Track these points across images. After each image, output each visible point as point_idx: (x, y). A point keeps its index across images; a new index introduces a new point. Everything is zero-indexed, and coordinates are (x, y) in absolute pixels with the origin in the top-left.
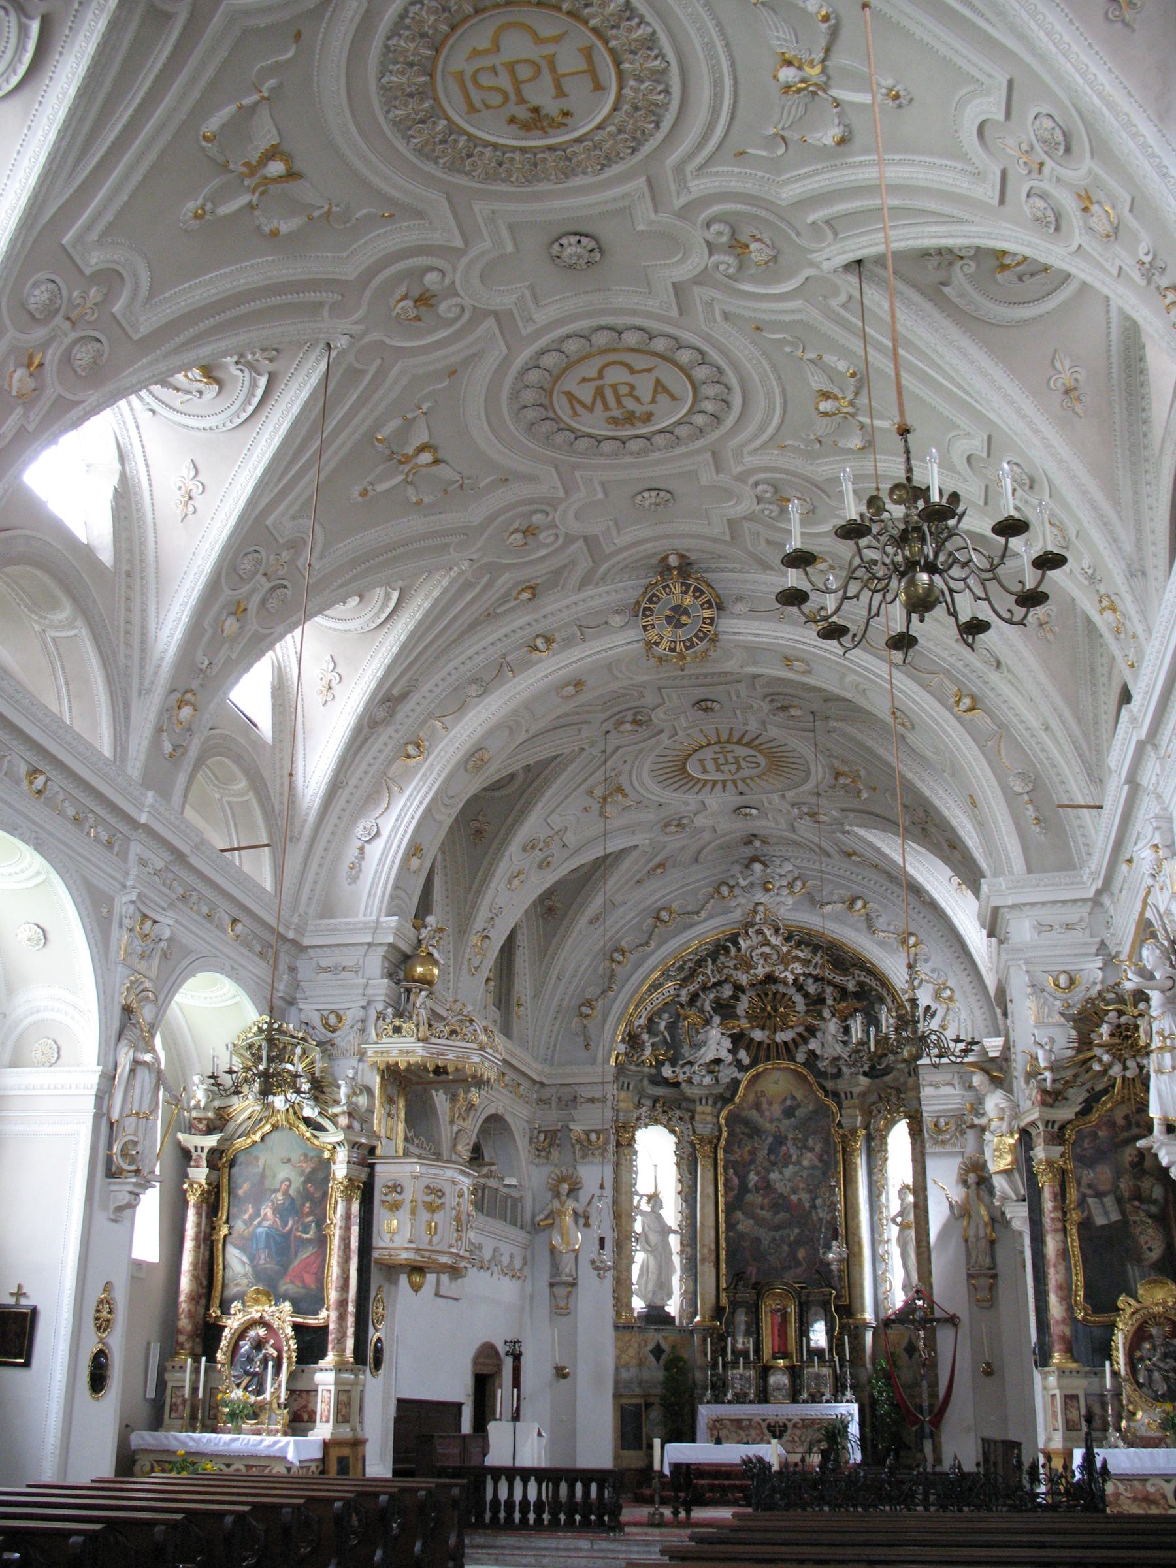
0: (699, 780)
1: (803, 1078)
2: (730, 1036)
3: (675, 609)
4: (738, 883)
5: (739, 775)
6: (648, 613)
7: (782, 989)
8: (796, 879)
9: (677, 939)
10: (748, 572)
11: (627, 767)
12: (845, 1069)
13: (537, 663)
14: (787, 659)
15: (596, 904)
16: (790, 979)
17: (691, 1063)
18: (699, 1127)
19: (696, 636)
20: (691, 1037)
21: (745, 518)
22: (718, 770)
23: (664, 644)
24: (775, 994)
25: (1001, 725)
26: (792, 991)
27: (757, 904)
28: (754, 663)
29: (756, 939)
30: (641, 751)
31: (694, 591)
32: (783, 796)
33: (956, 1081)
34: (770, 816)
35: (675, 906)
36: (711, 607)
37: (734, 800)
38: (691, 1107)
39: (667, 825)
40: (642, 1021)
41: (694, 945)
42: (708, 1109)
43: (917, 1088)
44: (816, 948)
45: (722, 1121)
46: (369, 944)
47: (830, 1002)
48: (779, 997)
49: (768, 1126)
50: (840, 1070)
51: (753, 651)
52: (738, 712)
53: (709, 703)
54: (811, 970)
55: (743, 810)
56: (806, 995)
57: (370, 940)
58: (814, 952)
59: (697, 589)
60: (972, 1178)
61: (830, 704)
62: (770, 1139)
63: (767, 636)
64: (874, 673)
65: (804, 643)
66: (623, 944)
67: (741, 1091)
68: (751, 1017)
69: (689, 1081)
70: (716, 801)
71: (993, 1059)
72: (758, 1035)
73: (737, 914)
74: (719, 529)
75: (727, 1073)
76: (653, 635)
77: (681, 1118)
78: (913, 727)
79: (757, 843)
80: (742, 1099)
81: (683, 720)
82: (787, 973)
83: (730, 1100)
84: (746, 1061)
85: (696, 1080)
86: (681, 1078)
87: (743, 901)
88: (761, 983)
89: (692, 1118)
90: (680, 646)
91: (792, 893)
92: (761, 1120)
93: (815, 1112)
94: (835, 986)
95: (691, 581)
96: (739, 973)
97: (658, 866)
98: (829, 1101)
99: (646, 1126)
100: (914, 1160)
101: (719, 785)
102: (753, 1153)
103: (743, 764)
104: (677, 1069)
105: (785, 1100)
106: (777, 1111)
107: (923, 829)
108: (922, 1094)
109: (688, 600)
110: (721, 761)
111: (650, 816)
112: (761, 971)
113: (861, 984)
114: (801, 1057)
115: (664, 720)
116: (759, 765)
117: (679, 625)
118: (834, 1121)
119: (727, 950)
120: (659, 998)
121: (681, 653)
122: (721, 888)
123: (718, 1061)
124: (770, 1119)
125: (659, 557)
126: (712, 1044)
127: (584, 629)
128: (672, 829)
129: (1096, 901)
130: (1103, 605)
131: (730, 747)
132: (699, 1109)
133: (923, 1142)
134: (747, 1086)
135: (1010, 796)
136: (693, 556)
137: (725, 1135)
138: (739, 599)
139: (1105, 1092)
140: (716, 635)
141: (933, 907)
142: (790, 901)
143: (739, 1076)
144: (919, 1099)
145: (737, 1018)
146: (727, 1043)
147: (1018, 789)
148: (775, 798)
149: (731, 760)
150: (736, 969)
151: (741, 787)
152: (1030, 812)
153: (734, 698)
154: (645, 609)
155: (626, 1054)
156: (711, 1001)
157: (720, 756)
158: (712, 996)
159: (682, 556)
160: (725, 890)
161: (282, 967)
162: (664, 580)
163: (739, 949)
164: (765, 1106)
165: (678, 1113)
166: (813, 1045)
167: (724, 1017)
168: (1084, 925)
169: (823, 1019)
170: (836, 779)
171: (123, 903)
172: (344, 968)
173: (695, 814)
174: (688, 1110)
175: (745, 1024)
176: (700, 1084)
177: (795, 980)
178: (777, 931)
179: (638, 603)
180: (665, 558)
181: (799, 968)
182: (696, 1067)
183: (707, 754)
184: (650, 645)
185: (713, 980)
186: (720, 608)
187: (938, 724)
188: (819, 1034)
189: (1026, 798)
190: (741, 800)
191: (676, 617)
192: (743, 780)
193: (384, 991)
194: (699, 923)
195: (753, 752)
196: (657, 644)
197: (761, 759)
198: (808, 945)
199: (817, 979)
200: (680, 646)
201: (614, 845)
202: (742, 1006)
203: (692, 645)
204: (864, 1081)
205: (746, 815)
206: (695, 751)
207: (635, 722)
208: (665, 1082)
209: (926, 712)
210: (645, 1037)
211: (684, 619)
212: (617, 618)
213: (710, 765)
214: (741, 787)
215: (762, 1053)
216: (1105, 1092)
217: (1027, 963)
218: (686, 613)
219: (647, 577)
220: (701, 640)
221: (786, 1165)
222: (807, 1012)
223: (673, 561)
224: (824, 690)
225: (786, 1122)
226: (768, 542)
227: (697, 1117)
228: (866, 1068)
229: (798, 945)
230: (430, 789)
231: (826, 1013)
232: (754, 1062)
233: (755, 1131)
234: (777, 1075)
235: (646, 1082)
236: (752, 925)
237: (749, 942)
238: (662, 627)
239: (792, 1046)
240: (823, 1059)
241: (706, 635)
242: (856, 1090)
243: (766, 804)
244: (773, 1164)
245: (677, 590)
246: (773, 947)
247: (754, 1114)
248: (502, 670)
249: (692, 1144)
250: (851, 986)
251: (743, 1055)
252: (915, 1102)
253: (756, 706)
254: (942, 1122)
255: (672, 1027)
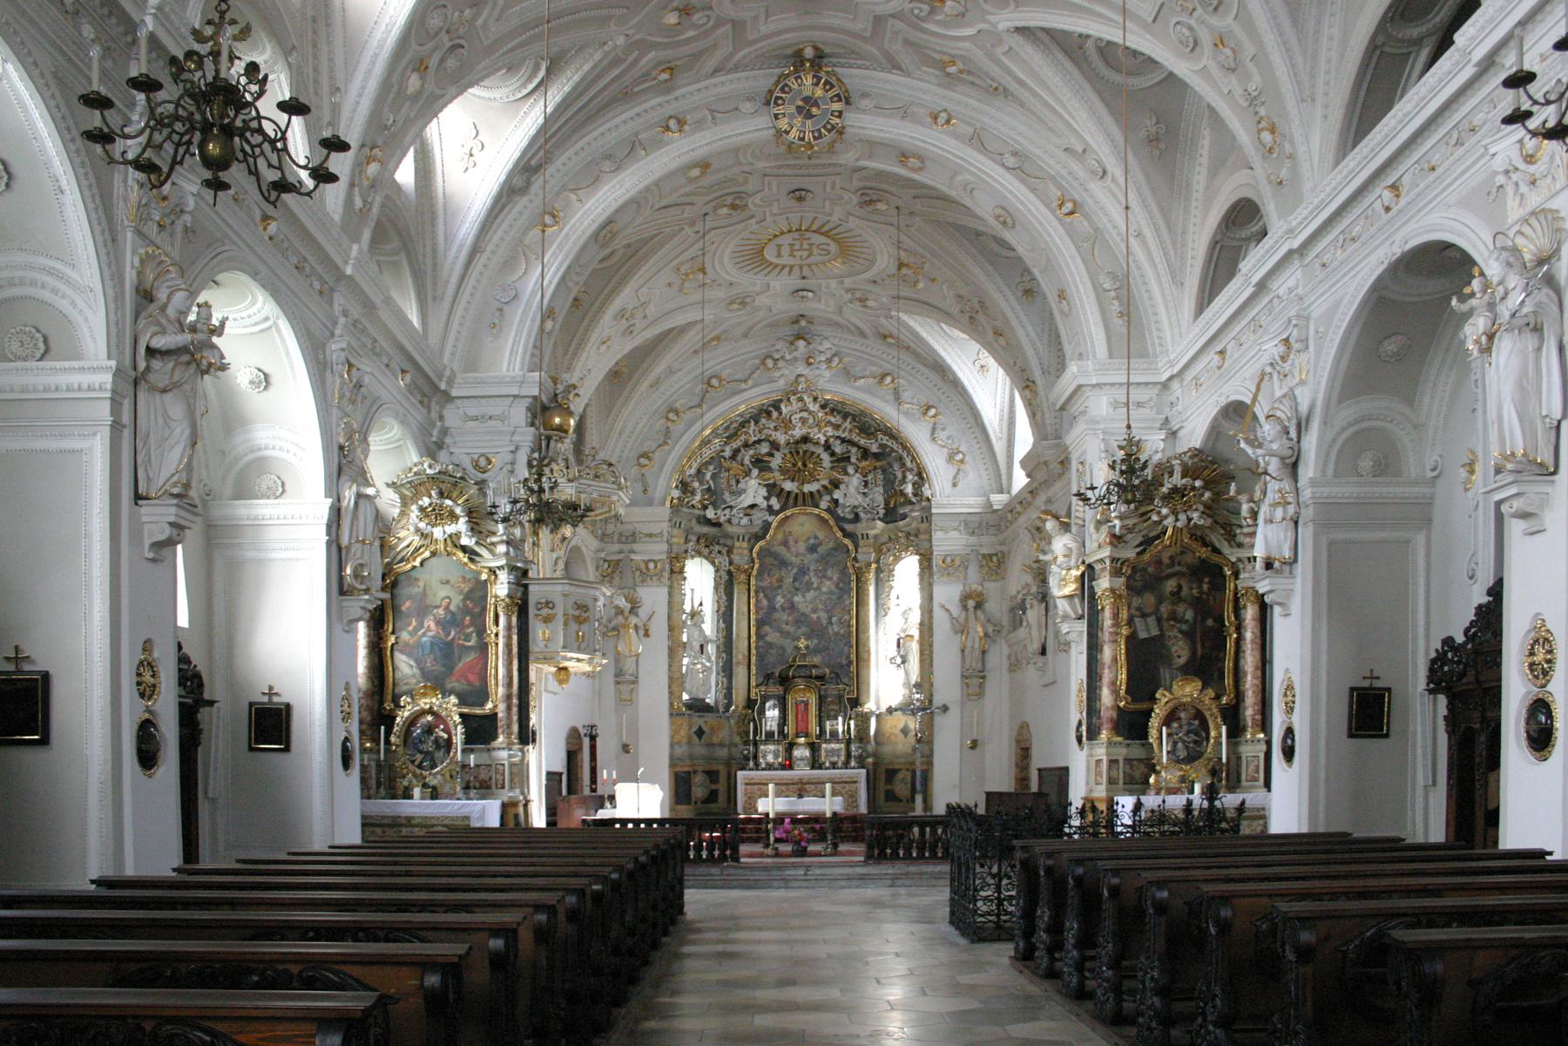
0: (771, 264)
1: (825, 521)
2: (766, 486)
3: (806, 100)
4: (783, 357)
5: (808, 261)
6: (780, 102)
7: (812, 448)
8: (834, 355)
9: (727, 402)
10: (875, 69)
11: (714, 246)
12: (862, 515)
13: (673, 142)
14: (903, 155)
15: (660, 368)
16: (823, 439)
17: (731, 507)
18: (736, 558)
19: (824, 127)
20: (730, 486)
21: (892, 16)
22: (792, 255)
23: (794, 134)
24: (805, 452)
25: (1097, 230)
26: (820, 450)
27: (799, 376)
28: (870, 157)
29: (796, 406)
30: (730, 233)
31: (825, 84)
32: (842, 282)
33: (962, 528)
34: (823, 298)
35: (724, 374)
36: (840, 100)
37: (794, 282)
38: (729, 542)
39: (731, 304)
40: (693, 471)
41: (742, 408)
42: (745, 545)
43: (929, 532)
44: (845, 417)
45: (754, 555)
46: (515, 396)
47: (853, 460)
48: (808, 454)
49: (794, 559)
50: (857, 515)
51: (873, 146)
52: (827, 203)
53: (803, 193)
54: (839, 433)
55: (801, 293)
56: (833, 454)
57: (516, 393)
58: (845, 417)
59: (826, 83)
60: (971, 603)
61: (918, 201)
62: (795, 570)
63: (890, 133)
64: (987, 175)
65: (924, 141)
66: (678, 405)
67: (771, 532)
68: (782, 470)
69: (729, 521)
70: (781, 283)
71: (996, 511)
72: (788, 486)
73: (781, 383)
74: (862, 25)
75: (759, 517)
76: (783, 124)
77: (719, 552)
78: (1014, 226)
79: (803, 323)
80: (772, 537)
81: (776, 204)
82: (820, 435)
83: (763, 537)
84: (777, 507)
85: (735, 521)
86: (722, 519)
87: (786, 372)
88: (797, 442)
89: (729, 552)
90: (809, 136)
91: (829, 368)
92: (788, 555)
93: (835, 549)
94: (859, 447)
95: (822, 74)
96: (778, 434)
97: (713, 339)
98: (846, 541)
99: (693, 557)
100: (922, 589)
101: (787, 269)
102: (780, 580)
103: (815, 251)
104: (719, 512)
105: (808, 539)
106: (802, 547)
107: (971, 317)
108: (934, 537)
109: (819, 92)
110: (796, 247)
111: (721, 294)
112: (798, 432)
113: (882, 446)
114: (824, 504)
115: (759, 206)
116: (829, 252)
117: (809, 116)
118: (849, 556)
119: (769, 414)
120: (707, 453)
121: (809, 142)
122: (767, 360)
123: (753, 506)
124: (796, 554)
125: (796, 48)
126: (751, 492)
127: (718, 112)
128: (735, 306)
129: (1165, 386)
130: (1261, 126)
131: (808, 235)
132: (737, 544)
133: (931, 575)
134: (777, 528)
135: (1099, 292)
136: (827, 50)
137: (757, 566)
138: (865, 95)
139: (1158, 537)
140: (843, 127)
141: (955, 384)
142: (827, 374)
143: (770, 519)
144: (930, 540)
145: (770, 469)
146: (764, 492)
147: (1107, 286)
148: (833, 283)
149: (805, 247)
150: (776, 429)
151: (806, 271)
152: (1116, 307)
153: (828, 189)
154: (777, 98)
155: (679, 498)
156: (752, 457)
157: (798, 242)
158: (751, 452)
159: (816, 48)
160: (770, 363)
161: (434, 415)
162: (796, 71)
163: (781, 413)
164: (791, 543)
165: (717, 548)
166: (837, 495)
167: (761, 470)
168: (1152, 404)
169: (846, 474)
170: (899, 269)
171: (336, 349)
172: (490, 418)
173: (758, 294)
174: (725, 545)
175: (777, 474)
176: (739, 524)
177: (826, 441)
178: (815, 399)
179: (771, 92)
180: (801, 50)
181: (830, 431)
182: (735, 511)
183: (786, 240)
184: (780, 133)
185: (754, 439)
186: (848, 102)
187: (1041, 223)
188: (842, 487)
189: (1113, 294)
190: (800, 283)
191: (806, 108)
192: (809, 266)
193: (531, 438)
194: (746, 390)
195: (828, 241)
196: (787, 132)
197: (833, 247)
198: (839, 412)
199: (843, 441)
200: (809, 136)
201: (680, 320)
202: (776, 462)
203: (820, 137)
204: (880, 524)
205: (803, 297)
206: (776, 236)
207: (733, 207)
208: (709, 522)
209: (1032, 214)
210: (696, 484)
211: (814, 110)
212: (748, 104)
213: (785, 250)
214: (805, 269)
215: (791, 501)
216: (1158, 537)
217: (1104, 432)
218: (816, 104)
219: (777, 67)
220: (829, 131)
221: (809, 591)
222: (832, 468)
223: (809, 53)
224: (934, 189)
225: (809, 556)
226: (907, 42)
227: (735, 551)
228: (881, 515)
229: (833, 410)
230: (567, 257)
231: (851, 470)
232: (782, 509)
233: (783, 563)
234: (802, 519)
235: (694, 521)
236: (795, 394)
237: (789, 408)
238: (792, 117)
239: (817, 496)
240: (844, 506)
241: (833, 127)
242: (872, 533)
243: (823, 289)
244: (797, 590)
245: (808, 80)
246: (810, 413)
247: (782, 550)
248: (633, 148)
249: (729, 573)
250: (874, 449)
251: (774, 502)
252: (926, 545)
253: (846, 198)
254: (949, 560)
255: (714, 477)
